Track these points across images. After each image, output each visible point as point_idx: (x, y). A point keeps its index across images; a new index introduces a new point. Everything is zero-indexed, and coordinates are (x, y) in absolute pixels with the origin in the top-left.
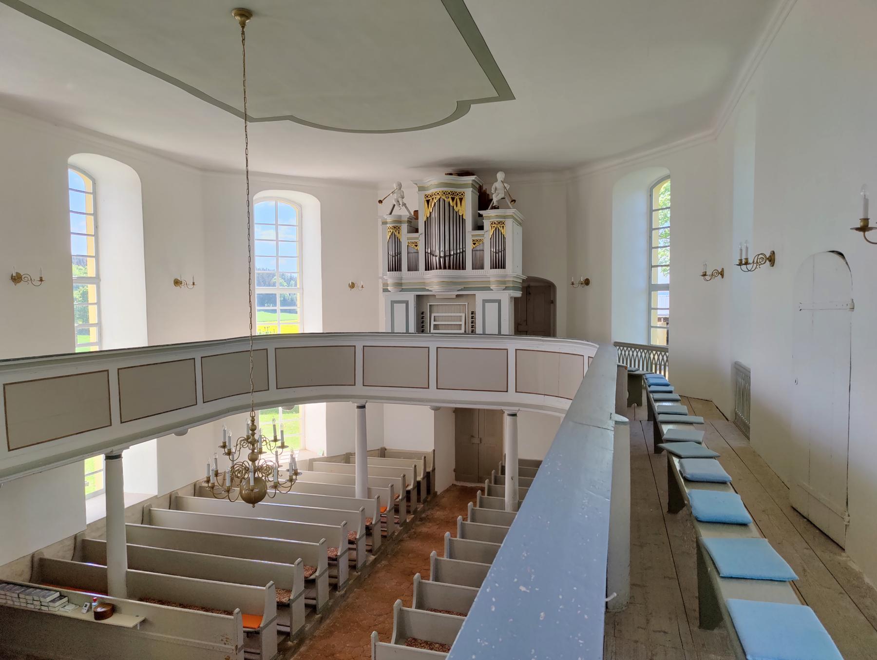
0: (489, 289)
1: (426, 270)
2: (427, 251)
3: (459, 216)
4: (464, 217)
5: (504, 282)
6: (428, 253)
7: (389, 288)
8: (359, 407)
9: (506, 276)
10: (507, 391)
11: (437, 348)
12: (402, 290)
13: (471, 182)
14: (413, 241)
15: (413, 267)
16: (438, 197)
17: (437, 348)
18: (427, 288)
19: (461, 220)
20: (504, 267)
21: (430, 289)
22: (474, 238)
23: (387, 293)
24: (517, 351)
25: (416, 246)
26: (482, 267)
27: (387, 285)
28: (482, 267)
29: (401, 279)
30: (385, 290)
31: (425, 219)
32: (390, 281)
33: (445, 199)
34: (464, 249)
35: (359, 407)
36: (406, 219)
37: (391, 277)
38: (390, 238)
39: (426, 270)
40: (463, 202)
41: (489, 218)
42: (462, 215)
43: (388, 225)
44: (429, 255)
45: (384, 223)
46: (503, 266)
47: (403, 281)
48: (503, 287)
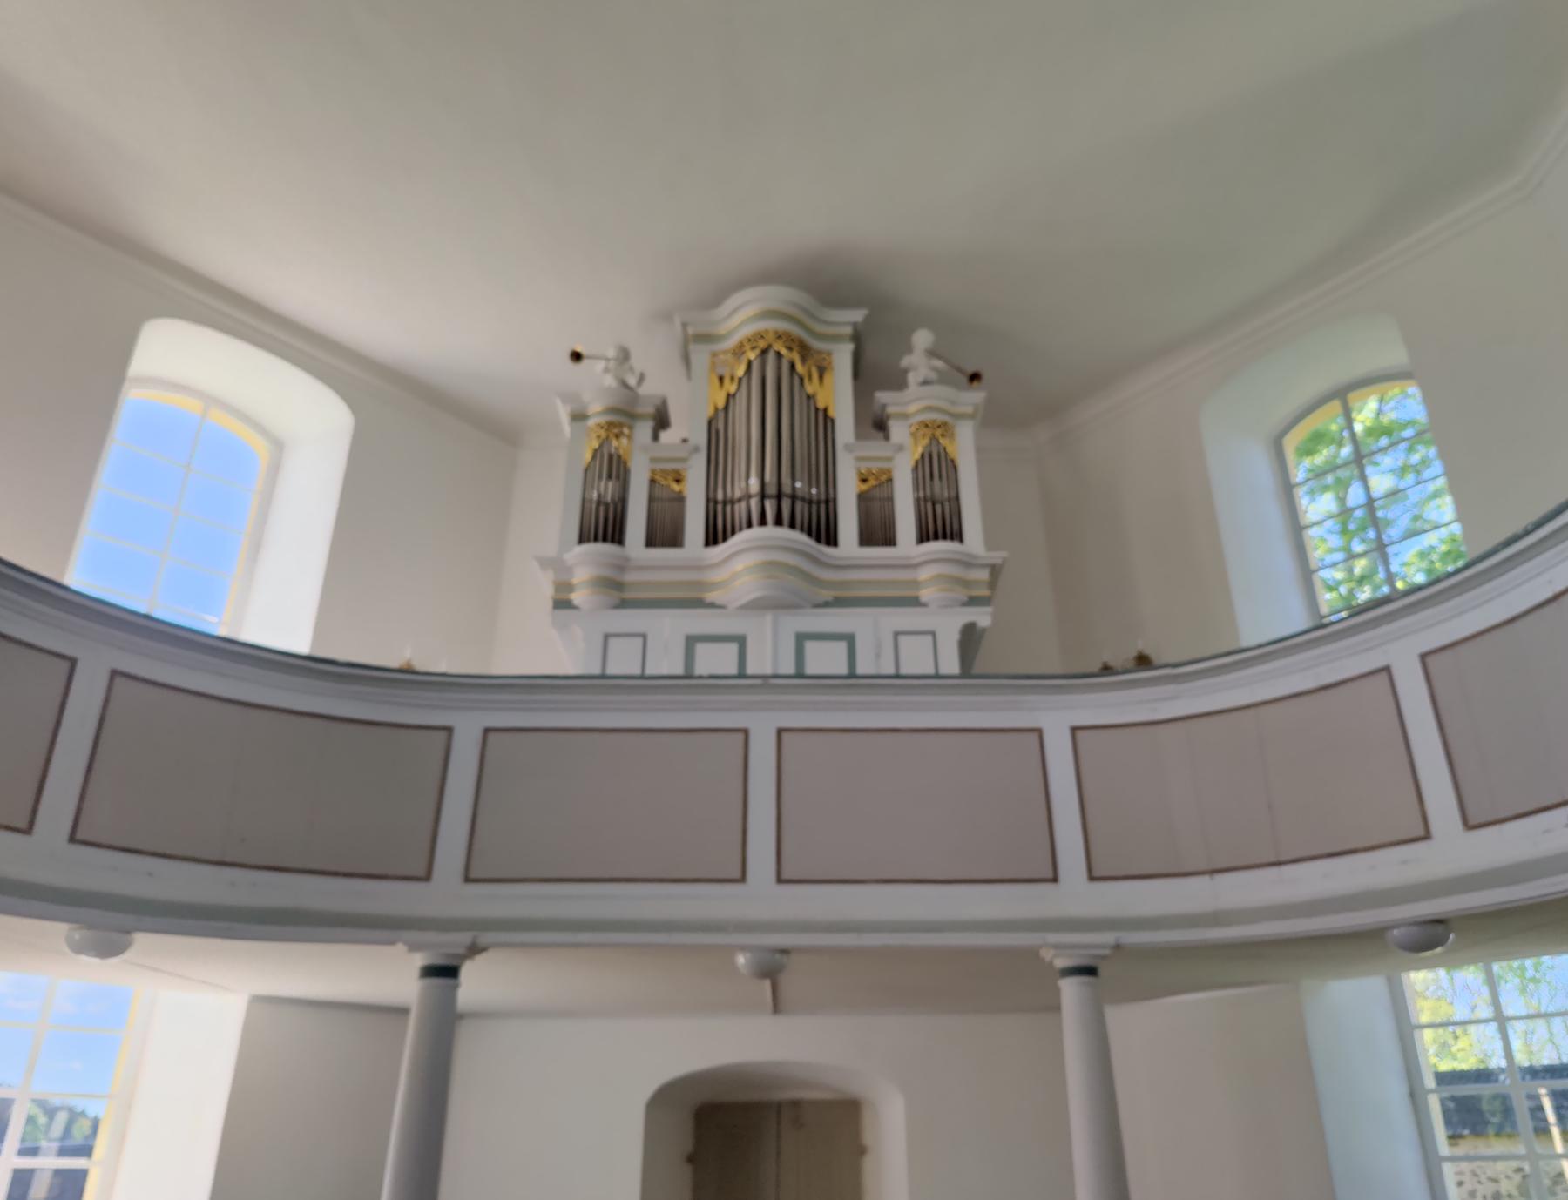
0: (915, 602)
1: (707, 544)
2: (711, 496)
3: (817, 410)
4: (831, 413)
5: (966, 583)
6: (716, 502)
7: (577, 597)
8: (431, 972)
9: (968, 563)
10: (1055, 880)
11: (780, 731)
12: (623, 604)
13: (848, 330)
14: (669, 466)
15: (664, 533)
16: (762, 344)
17: (780, 731)
18: (710, 597)
19: (826, 421)
20: (961, 540)
21: (718, 602)
22: (864, 467)
23: (564, 614)
24: (1080, 734)
25: (678, 481)
26: (889, 540)
27: (570, 587)
28: (889, 540)
29: (622, 566)
30: (562, 604)
31: (711, 411)
32: (581, 575)
33: (784, 351)
34: (831, 496)
35: (431, 972)
36: (650, 410)
37: (587, 560)
38: (594, 457)
39: (707, 544)
40: (827, 378)
41: (905, 416)
42: (825, 410)
43: (591, 422)
44: (720, 508)
45: (579, 417)
46: (956, 535)
47: (630, 577)
48: (962, 594)
